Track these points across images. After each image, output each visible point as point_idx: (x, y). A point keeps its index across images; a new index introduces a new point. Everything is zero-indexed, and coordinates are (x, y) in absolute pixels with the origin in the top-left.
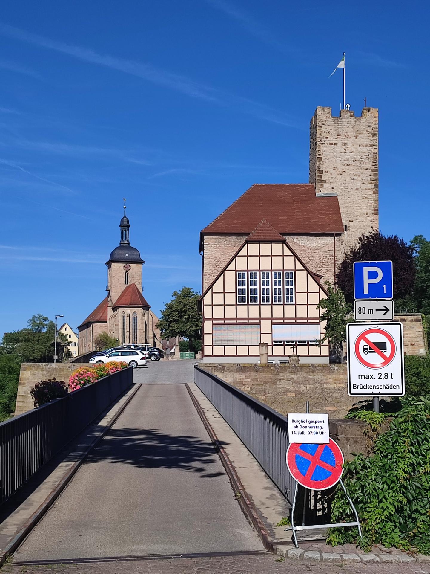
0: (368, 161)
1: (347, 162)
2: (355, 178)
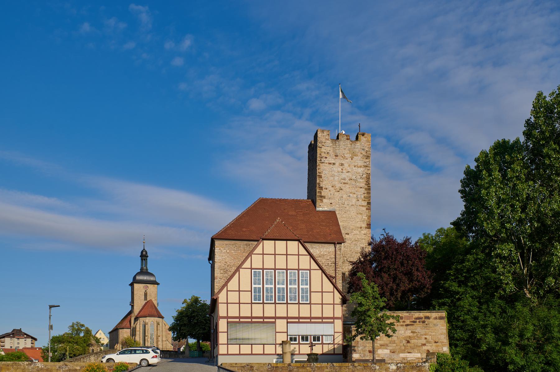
0: (361, 180)
1: (344, 181)
2: (351, 195)
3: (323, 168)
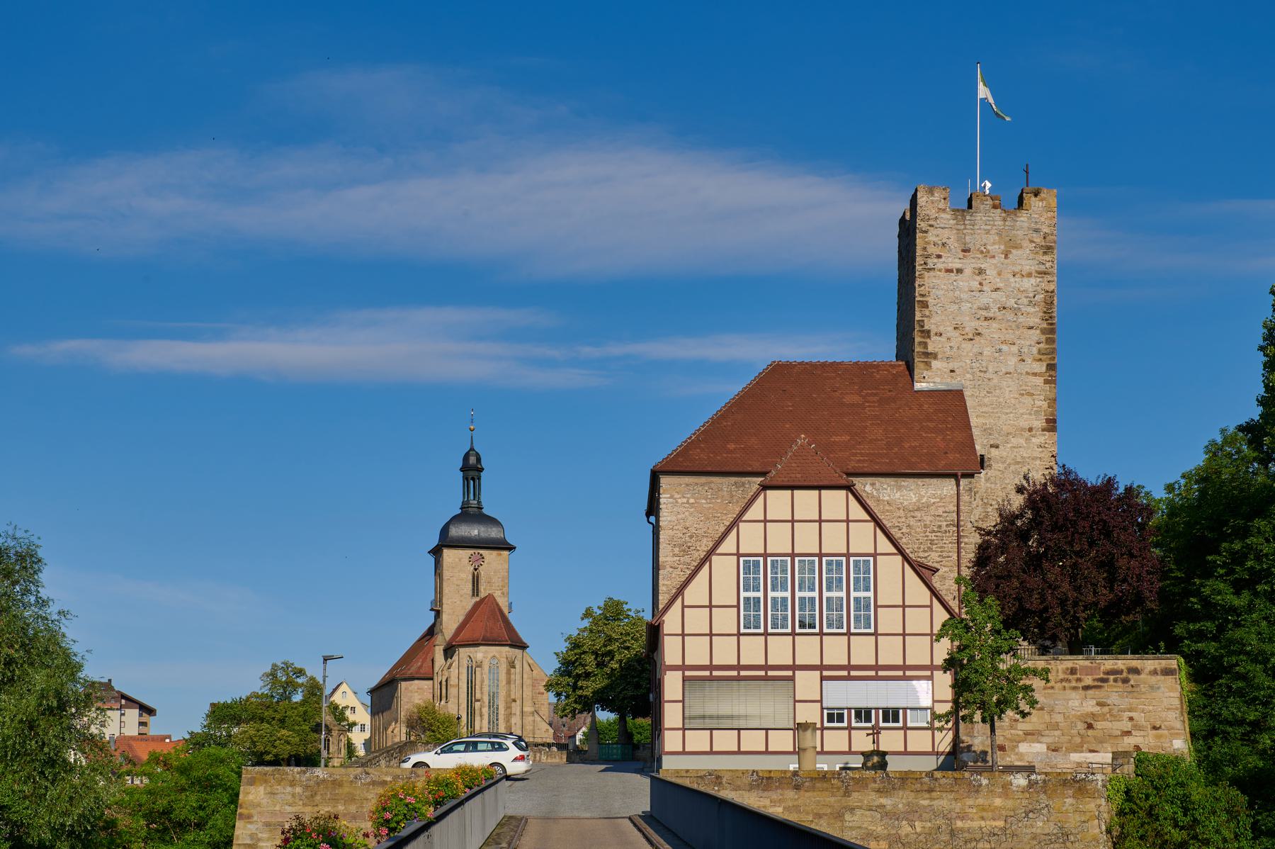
0: (1031, 310)
1: (985, 313)
3: (931, 284)
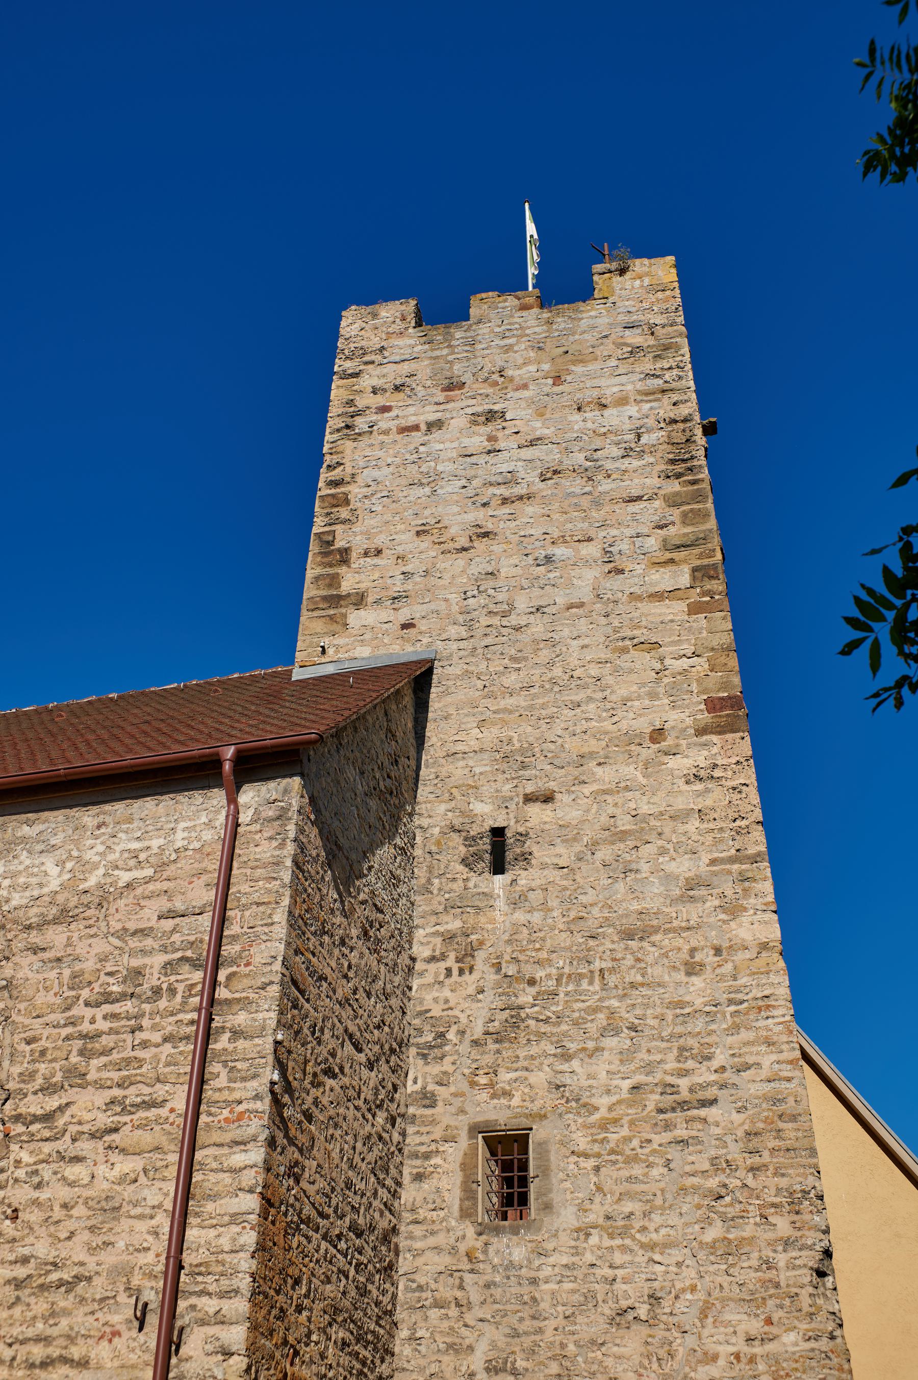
2: (560, 551)
